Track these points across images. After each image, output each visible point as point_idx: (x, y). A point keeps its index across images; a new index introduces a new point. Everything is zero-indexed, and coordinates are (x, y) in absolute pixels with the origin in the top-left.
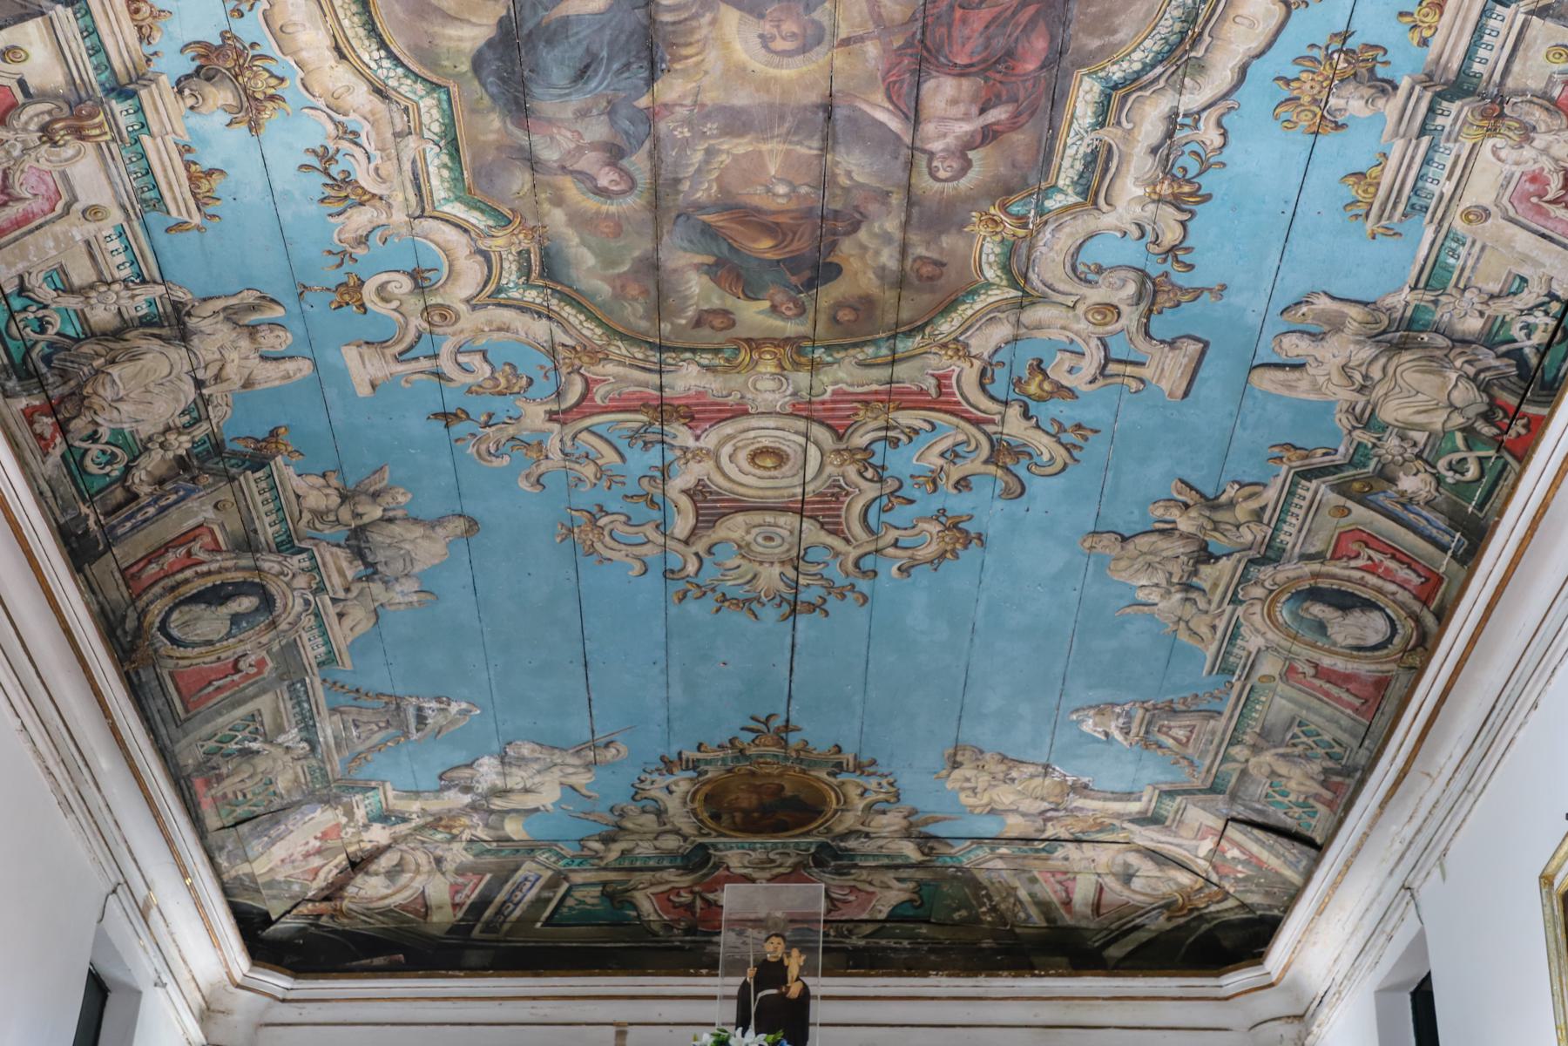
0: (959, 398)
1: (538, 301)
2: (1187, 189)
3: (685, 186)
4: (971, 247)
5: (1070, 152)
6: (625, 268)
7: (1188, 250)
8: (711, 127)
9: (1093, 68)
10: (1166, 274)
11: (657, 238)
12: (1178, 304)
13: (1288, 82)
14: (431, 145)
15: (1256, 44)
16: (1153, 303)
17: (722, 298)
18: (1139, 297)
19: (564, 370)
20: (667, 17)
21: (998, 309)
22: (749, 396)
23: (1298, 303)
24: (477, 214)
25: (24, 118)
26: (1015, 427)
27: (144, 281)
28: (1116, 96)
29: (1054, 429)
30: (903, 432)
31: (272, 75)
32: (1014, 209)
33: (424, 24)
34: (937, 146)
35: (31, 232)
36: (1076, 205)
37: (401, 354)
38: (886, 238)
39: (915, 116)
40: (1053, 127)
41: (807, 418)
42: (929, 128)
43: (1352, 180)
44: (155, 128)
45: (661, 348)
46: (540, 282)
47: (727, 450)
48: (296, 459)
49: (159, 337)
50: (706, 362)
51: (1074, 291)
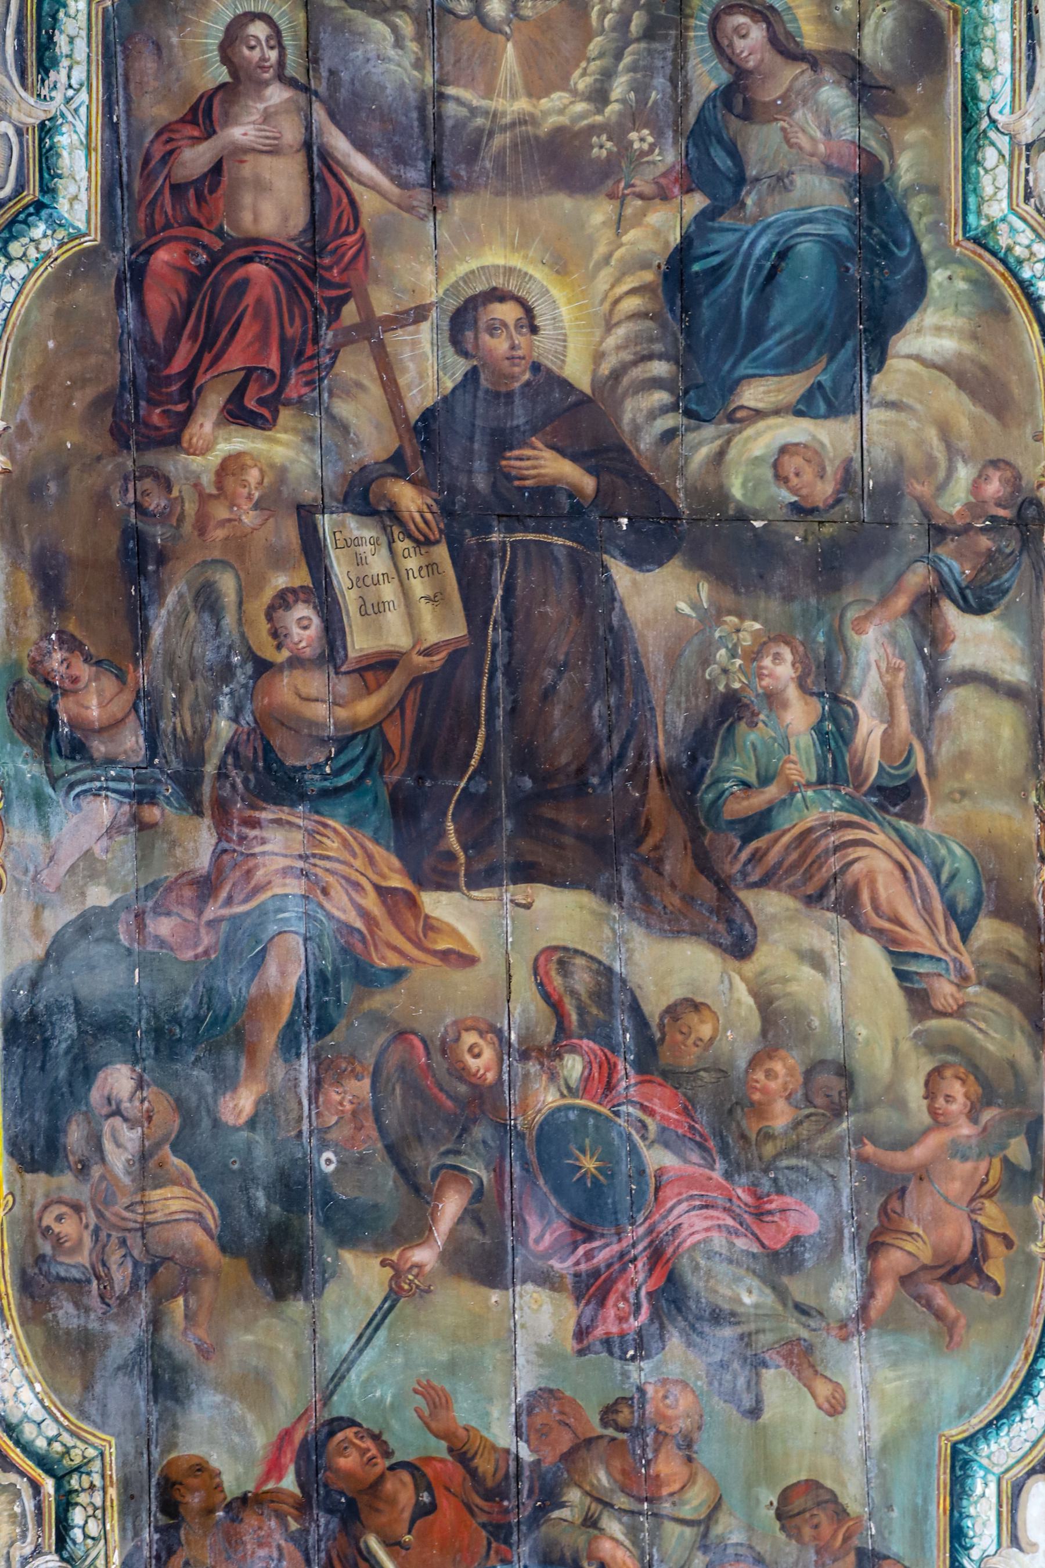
8: (602, 148)
20: (660, 368)
34: (277, 95)
42: (291, 133)
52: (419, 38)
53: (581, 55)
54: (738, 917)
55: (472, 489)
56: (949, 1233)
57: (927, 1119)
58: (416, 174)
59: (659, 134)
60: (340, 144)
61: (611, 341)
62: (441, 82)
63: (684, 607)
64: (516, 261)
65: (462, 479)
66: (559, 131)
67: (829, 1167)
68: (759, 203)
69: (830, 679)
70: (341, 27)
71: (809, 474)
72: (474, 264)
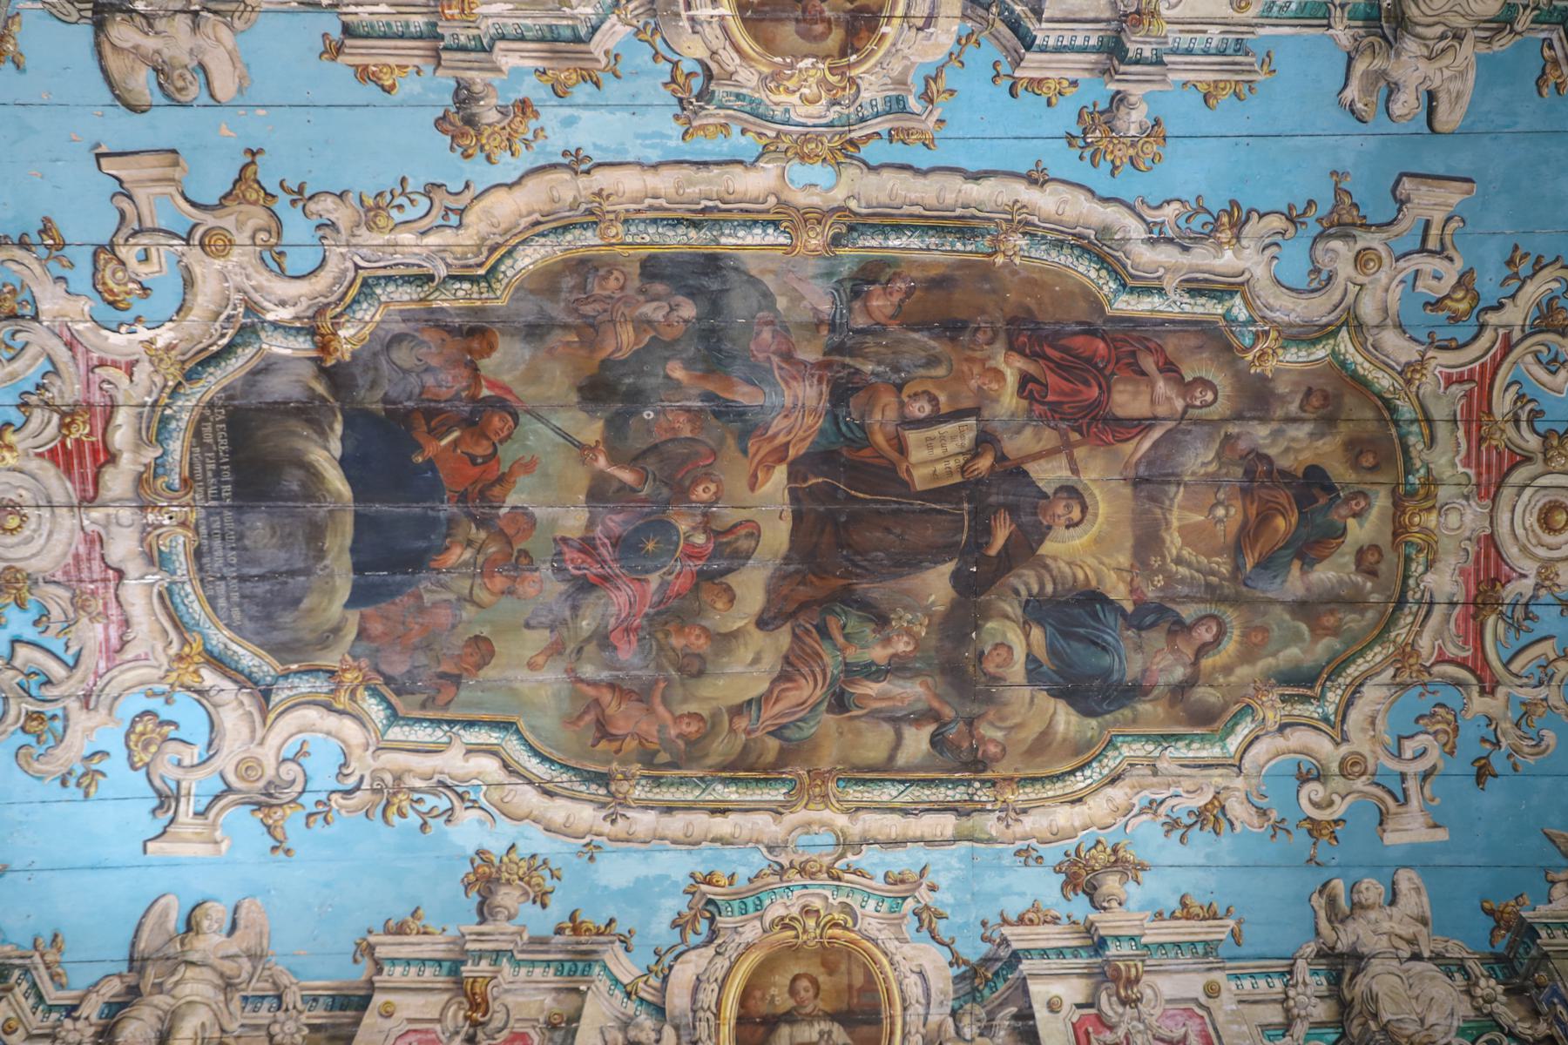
0: (1477, 365)
1: (1339, 692)
2: (1225, 219)
3: (1214, 580)
4: (1289, 371)
5: (1187, 308)
6: (1304, 627)
7: (1291, 207)
8: (1155, 562)
9: (1105, 302)
10: (1319, 220)
11: (1271, 602)
12: (1355, 205)
13: (1115, 168)
14: (1167, 753)
15: (1082, 196)
16: (1354, 225)
17: (1343, 555)
18: (1347, 237)
19: (1426, 678)
20: (1049, 588)
21: (1363, 344)
22: (1467, 534)
23: (1353, 112)
24: (1239, 728)
25: (1110, 1013)
26: (1515, 315)
27: (1291, 973)
28: (1131, 283)
29: (1515, 284)
30: (1522, 408)
31: (1095, 847)
32: (1248, 341)
33: (1055, 745)
34: (1179, 404)
35: (1219, 1037)
36: (1244, 298)
37: (1396, 799)
38: (1276, 434)
39: (1142, 425)
40: (1163, 322)
41: (1499, 487)
42: (1161, 410)
43: (1212, 101)
44: (1136, 932)
45: (1401, 602)
46: (1318, 690)
47: (1542, 552)
48: (1527, 900)
49: (1353, 976)
50: (1421, 569)
51: (1342, 288)
52: (1206, 474)
53: (1199, 552)
54: (778, 622)
55: (990, 495)
56: (621, 723)
57: (678, 713)
58: (1142, 471)
59: (1162, 589)
60: (1156, 434)
61: (1062, 565)
62: (1186, 485)
63: (932, 598)
64: (1100, 519)
65: (994, 490)
66: (1163, 541)
67: (652, 665)
68: (1128, 638)
69: (897, 669)
70: (1211, 436)
71: (998, 660)
72: (1099, 498)
